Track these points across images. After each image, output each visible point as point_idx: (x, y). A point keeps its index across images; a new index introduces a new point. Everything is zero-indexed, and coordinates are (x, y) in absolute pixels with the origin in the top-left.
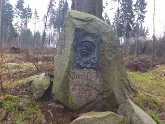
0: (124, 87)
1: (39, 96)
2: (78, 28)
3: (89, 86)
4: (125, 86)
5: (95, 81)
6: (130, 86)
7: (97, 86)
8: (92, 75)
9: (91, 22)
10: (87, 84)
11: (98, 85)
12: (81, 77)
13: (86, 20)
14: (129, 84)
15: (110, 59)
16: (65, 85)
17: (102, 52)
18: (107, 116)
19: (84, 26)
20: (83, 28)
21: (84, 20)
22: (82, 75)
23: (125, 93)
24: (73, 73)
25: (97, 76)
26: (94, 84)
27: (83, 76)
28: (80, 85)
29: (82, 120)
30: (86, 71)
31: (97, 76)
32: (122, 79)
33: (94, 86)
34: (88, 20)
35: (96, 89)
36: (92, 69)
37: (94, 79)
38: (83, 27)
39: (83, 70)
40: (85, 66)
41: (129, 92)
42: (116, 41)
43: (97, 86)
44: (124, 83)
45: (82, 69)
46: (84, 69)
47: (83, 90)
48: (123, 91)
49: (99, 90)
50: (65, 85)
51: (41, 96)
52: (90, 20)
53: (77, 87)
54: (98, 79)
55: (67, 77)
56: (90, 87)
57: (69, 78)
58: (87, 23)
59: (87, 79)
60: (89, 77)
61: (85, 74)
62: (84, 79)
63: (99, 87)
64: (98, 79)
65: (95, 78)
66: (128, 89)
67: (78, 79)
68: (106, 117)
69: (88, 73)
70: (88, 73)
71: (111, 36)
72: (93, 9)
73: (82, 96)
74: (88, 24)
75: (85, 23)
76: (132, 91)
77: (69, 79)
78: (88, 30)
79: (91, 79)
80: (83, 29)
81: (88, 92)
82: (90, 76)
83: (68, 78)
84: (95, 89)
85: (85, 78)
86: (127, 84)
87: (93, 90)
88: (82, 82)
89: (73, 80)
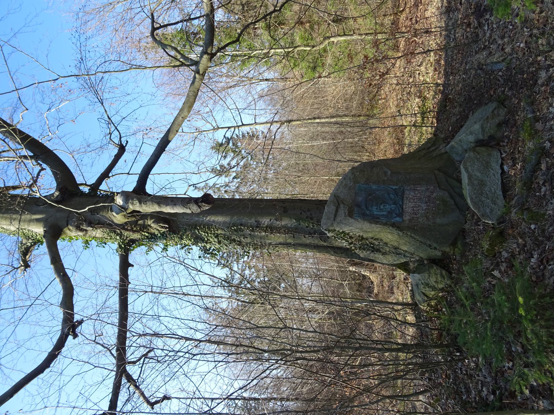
1: (446, 277)
2: (349, 213)
3: (429, 200)
5: (422, 192)
6: (429, 148)
7: (428, 189)
12: (415, 211)
13: (337, 204)
14: (424, 149)
15: (389, 172)
18: (467, 171)
20: (348, 208)
22: (413, 210)
25: (414, 189)
27: (415, 209)
28: (427, 212)
29: (471, 199)
31: (414, 189)
32: (417, 159)
33: (428, 194)
35: (432, 191)
39: (406, 208)
40: (400, 205)
41: (436, 149)
43: (428, 189)
46: (404, 207)
49: (434, 187)
53: (430, 216)
54: (419, 189)
58: (340, 203)
62: (419, 206)
66: (433, 151)
68: (468, 171)
72: (302, 212)
75: (342, 206)
82: (414, 200)
84: (432, 193)
88: (423, 210)
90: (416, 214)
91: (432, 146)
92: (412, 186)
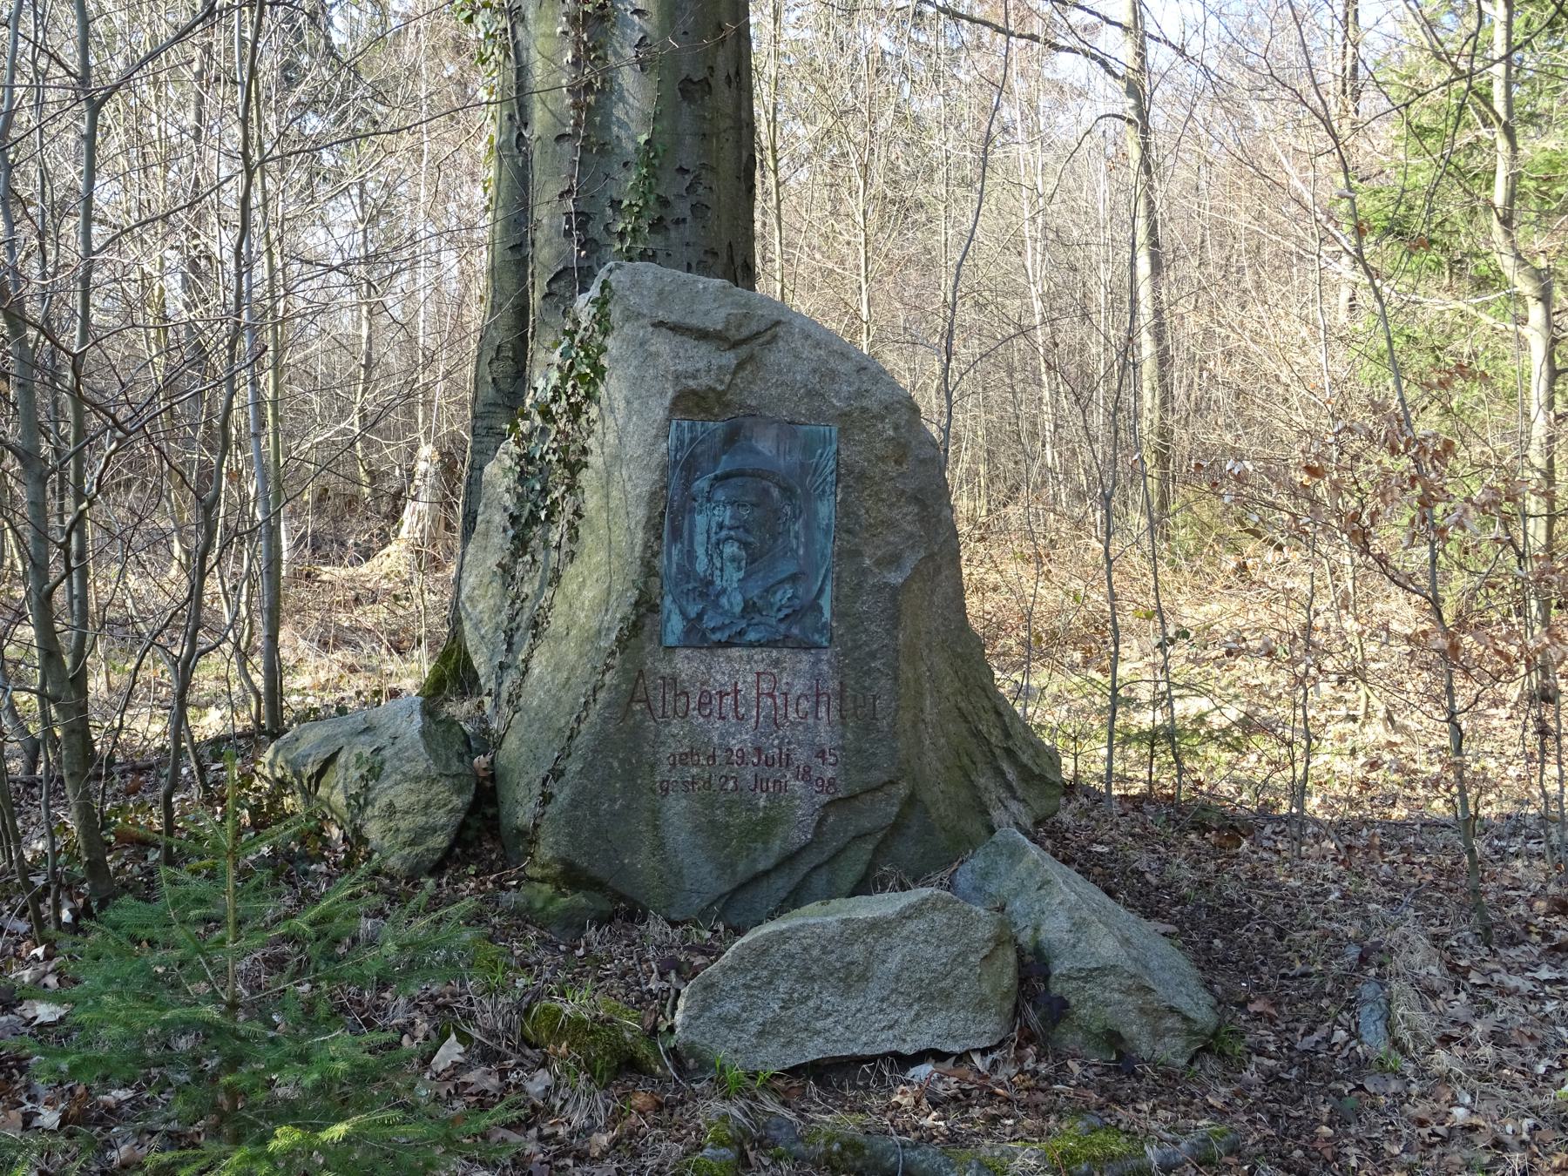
0: (978, 757)
1: (419, 849)
2: (694, 392)
4: (983, 753)
5: (807, 728)
6: (1010, 753)
7: (821, 754)
8: (784, 688)
9: (769, 342)
10: (758, 750)
11: (823, 752)
12: (715, 702)
13: (734, 335)
15: (895, 578)
16: (616, 764)
18: (904, 916)
19: (728, 378)
20: (720, 388)
21: (726, 339)
22: (722, 694)
23: (985, 798)
24: (663, 678)
25: (818, 695)
26: (800, 744)
27: (728, 700)
29: (783, 937)
31: (818, 695)
33: (801, 756)
34: (745, 332)
35: (815, 774)
36: (785, 651)
38: (722, 382)
39: (729, 659)
40: (741, 633)
41: (1009, 787)
42: (923, 462)
43: (821, 754)
44: (977, 734)
45: (720, 651)
46: (735, 652)
47: (731, 784)
48: (973, 786)
49: (832, 782)
50: (616, 764)
51: (435, 850)
52: (758, 334)
53: (695, 771)
54: (823, 709)
55: (628, 711)
57: (642, 712)
58: (744, 351)
59: (754, 713)
60: (770, 701)
61: (740, 686)
62: (740, 718)
63: (832, 759)
64: (823, 709)
65: (804, 705)
67: (701, 720)
68: (909, 918)
69: (758, 674)
70: (758, 674)
71: (891, 433)
72: (688, 178)
73: (727, 826)
74: (751, 358)
75: (730, 359)
76: (1025, 780)
77: (642, 721)
78: (754, 403)
79: (782, 712)
80: (724, 393)
82: (771, 695)
83: (634, 713)
84: (806, 775)
85: (742, 710)
86: (993, 740)
87: (797, 785)
88: (722, 736)
89: (669, 724)
90: (701, 705)
91: (1023, 770)
92: (834, 685)
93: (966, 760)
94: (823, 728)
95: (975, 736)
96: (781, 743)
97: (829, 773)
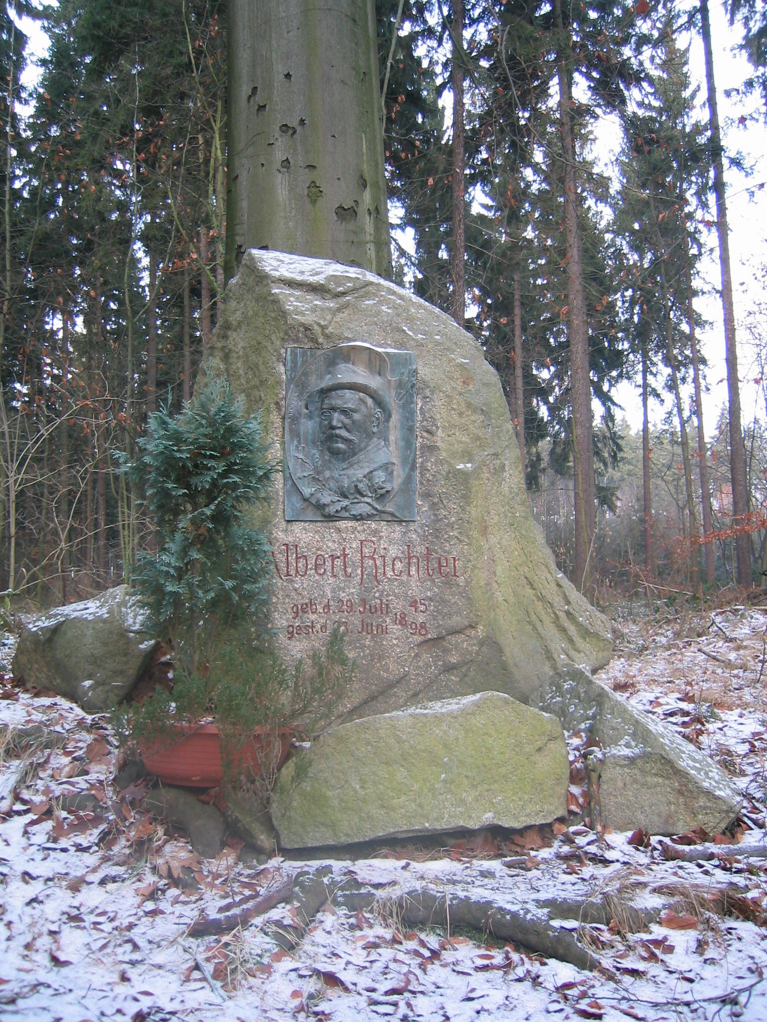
3: (373, 610)
4: (547, 613)
5: (402, 583)
7: (414, 604)
8: (382, 552)
12: (328, 564)
17: (425, 434)
24: (286, 545)
25: (410, 558)
26: (397, 597)
27: (338, 562)
28: (328, 606)
30: (353, 533)
31: (410, 558)
33: (397, 605)
37: (393, 570)
40: (345, 509)
41: (571, 641)
43: (414, 604)
44: (541, 598)
46: (342, 524)
48: (540, 636)
49: (423, 626)
52: (354, 290)
53: (313, 617)
54: (413, 571)
56: (376, 611)
59: (359, 572)
60: (371, 562)
61: (347, 551)
63: (422, 608)
64: (413, 571)
65: (399, 565)
66: (563, 630)
67: (317, 577)
69: (362, 542)
70: (362, 542)
81: (369, 636)
84: (402, 621)
85: (349, 570)
87: (395, 628)
89: (292, 581)
90: (317, 566)
91: (578, 625)
92: (420, 550)
93: (534, 617)
94: (414, 583)
95: (539, 599)
96: (381, 595)
97: (421, 618)
